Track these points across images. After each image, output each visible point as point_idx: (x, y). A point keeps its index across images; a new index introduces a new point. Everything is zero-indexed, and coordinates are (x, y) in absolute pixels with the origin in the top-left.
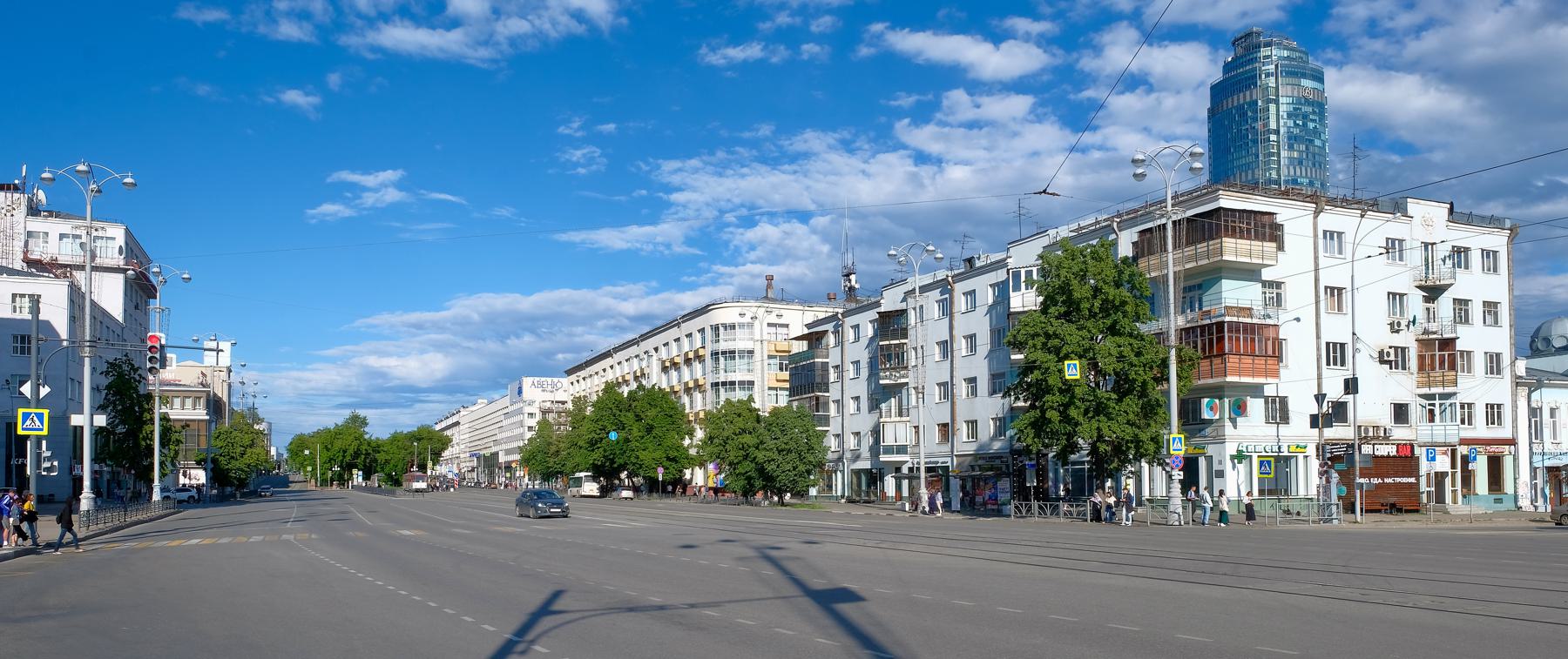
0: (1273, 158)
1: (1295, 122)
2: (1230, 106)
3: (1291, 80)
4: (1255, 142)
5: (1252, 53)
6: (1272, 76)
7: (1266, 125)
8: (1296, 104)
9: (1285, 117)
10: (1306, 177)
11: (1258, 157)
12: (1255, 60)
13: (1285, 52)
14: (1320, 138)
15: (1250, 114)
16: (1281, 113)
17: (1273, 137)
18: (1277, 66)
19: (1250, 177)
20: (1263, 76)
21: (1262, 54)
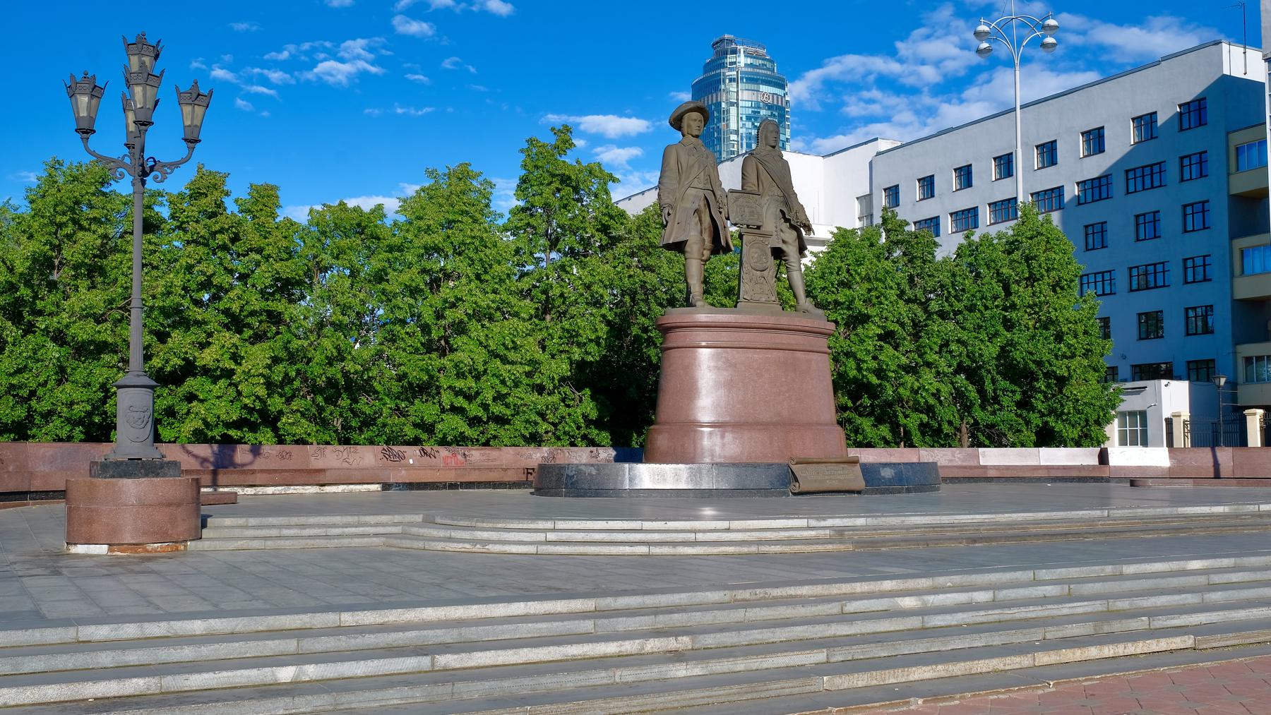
1: (753, 124)
2: (710, 103)
4: (719, 139)
6: (734, 81)
7: (728, 126)
8: (755, 108)
9: (744, 119)
12: (723, 66)
15: (716, 114)
16: (740, 116)
17: (733, 137)
21: (728, 60)
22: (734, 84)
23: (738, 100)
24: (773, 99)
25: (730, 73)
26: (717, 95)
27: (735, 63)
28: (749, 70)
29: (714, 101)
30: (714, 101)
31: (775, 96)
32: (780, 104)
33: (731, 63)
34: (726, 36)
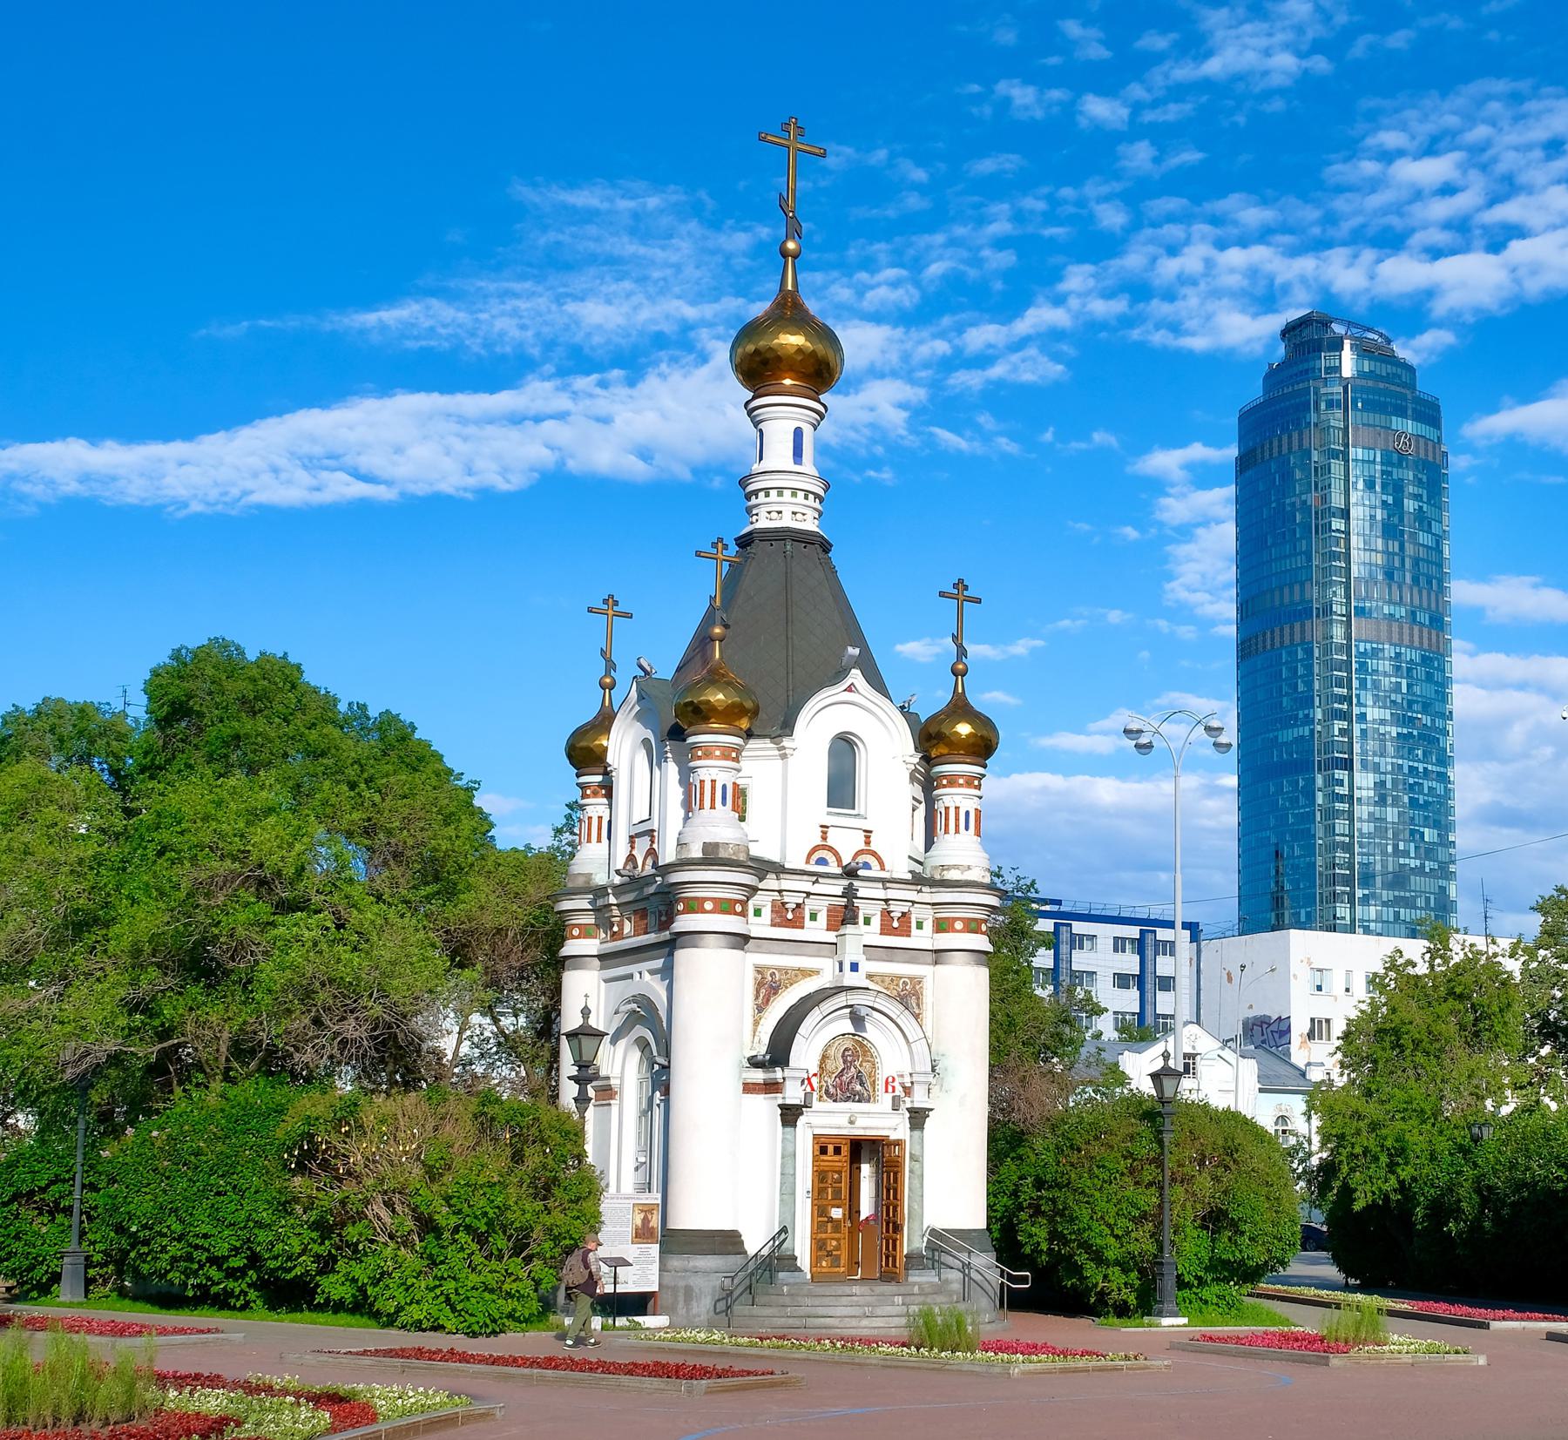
0: (1338, 564)
5: (1307, 361)
6: (1339, 406)
7: (1325, 499)
10: (1401, 602)
11: (1310, 559)
14: (1429, 531)
15: (1298, 475)
19: (1297, 598)
20: (1323, 406)
23: (1346, 445)
24: (1417, 447)
26: (1301, 435)
28: (1370, 383)
31: (1422, 441)
32: (1430, 459)
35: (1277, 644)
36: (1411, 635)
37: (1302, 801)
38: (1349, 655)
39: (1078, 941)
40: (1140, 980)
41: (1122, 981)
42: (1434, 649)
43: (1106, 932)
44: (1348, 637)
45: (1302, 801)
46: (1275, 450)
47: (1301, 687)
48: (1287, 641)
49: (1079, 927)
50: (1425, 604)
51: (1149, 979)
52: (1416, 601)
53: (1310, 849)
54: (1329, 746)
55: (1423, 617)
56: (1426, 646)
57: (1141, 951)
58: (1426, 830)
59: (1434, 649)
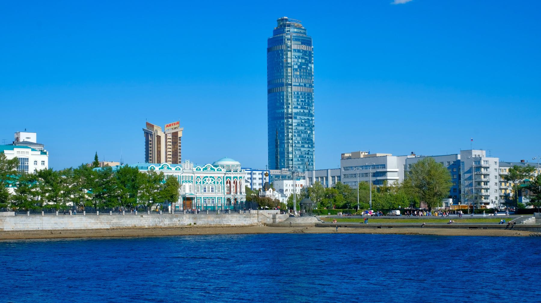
3: (296, 42)
9: (294, 58)
13: (296, 29)
15: (281, 55)
18: (291, 36)
19: (281, 82)
20: (286, 40)
21: (286, 30)
22: (290, 41)
25: (287, 36)
26: (281, 46)
27: (289, 31)
29: (280, 49)
30: (280, 49)
33: (287, 31)
34: (285, 17)
35: (276, 91)
36: (305, 89)
37: (282, 125)
38: (292, 94)
39: (254, 174)
40: (262, 179)
41: (260, 179)
42: (310, 92)
43: (257, 172)
44: (292, 90)
45: (282, 125)
46: (276, 49)
47: (281, 101)
48: (278, 91)
49: (254, 172)
50: (308, 82)
51: (263, 178)
52: (306, 82)
53: (284, 136)
54: (288, 114)
55: (307, 85)
56: (308, 91)
57: (262, 175)
58: (308, 131)
59: (310, 92)
